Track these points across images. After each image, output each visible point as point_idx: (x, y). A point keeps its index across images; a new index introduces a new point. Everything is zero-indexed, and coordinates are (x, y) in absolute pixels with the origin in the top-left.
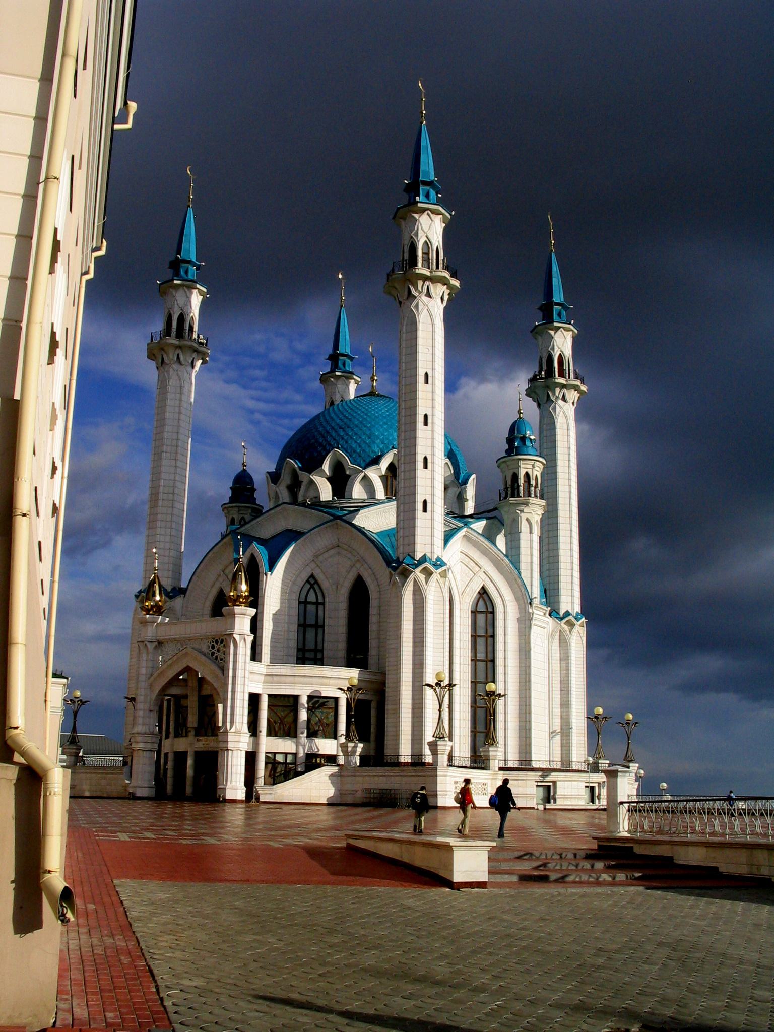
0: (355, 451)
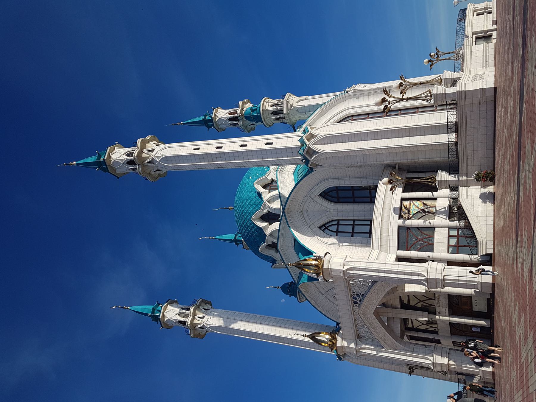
0: (255, 208)
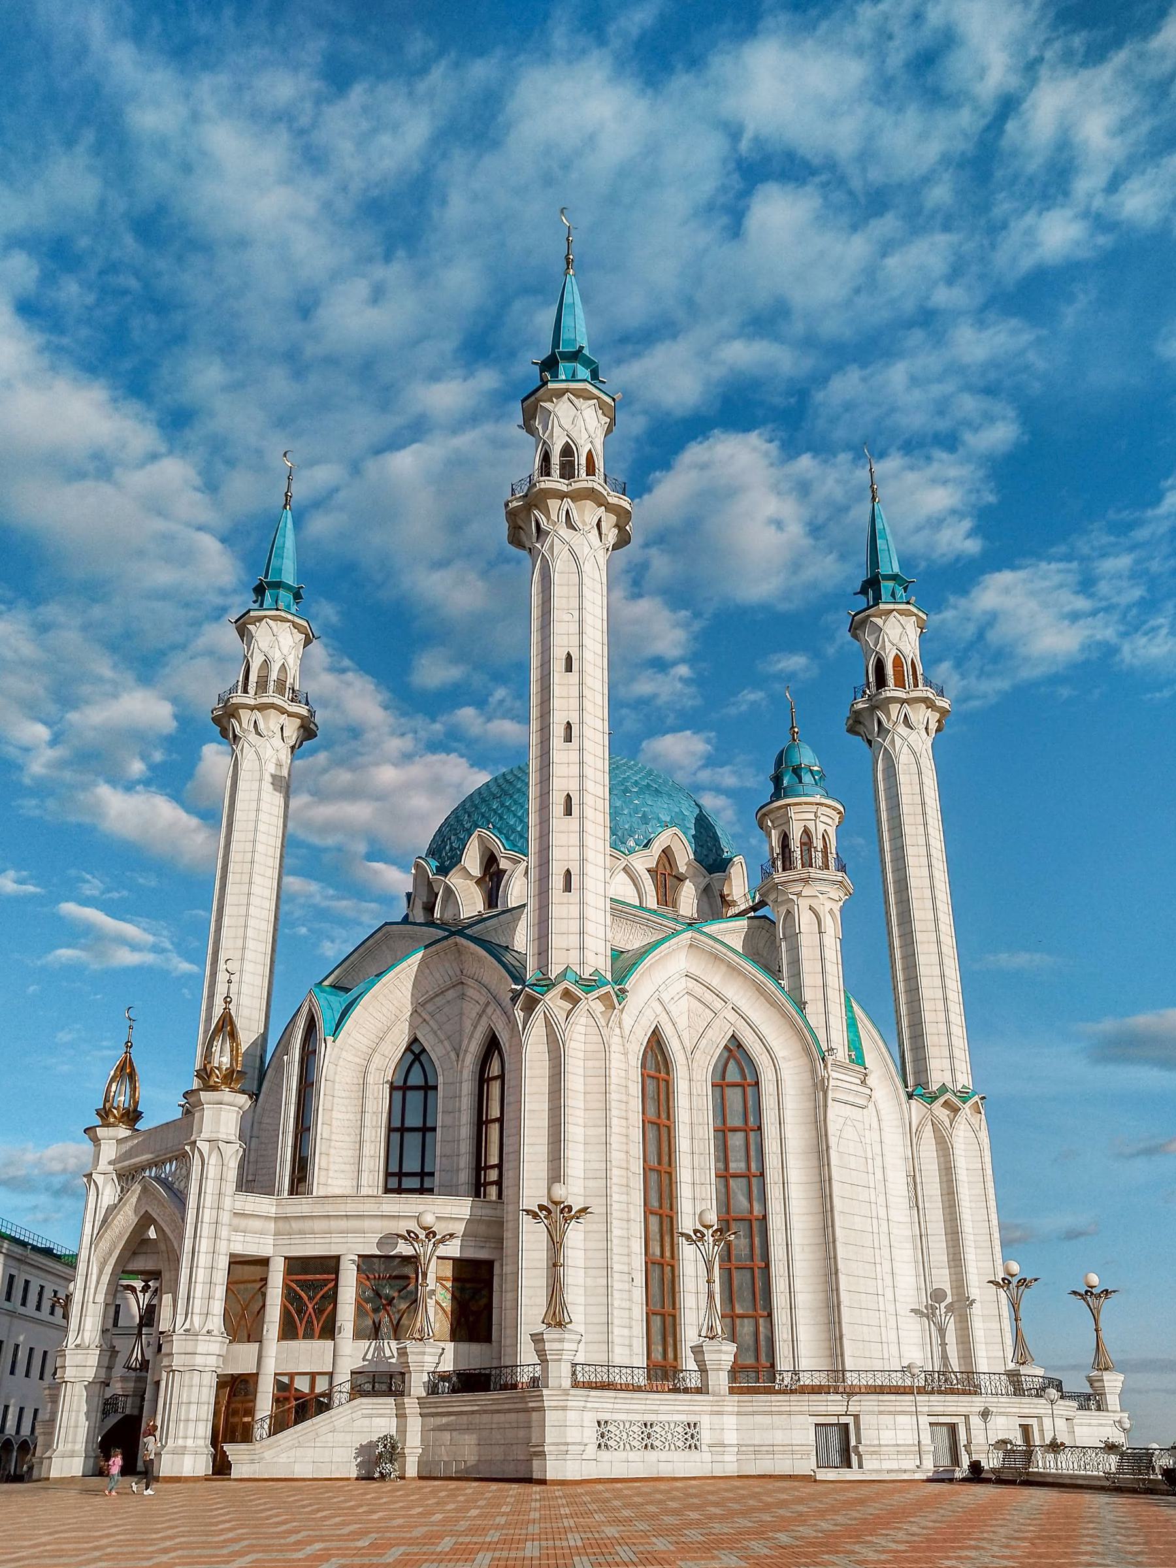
0: (514, 831)
